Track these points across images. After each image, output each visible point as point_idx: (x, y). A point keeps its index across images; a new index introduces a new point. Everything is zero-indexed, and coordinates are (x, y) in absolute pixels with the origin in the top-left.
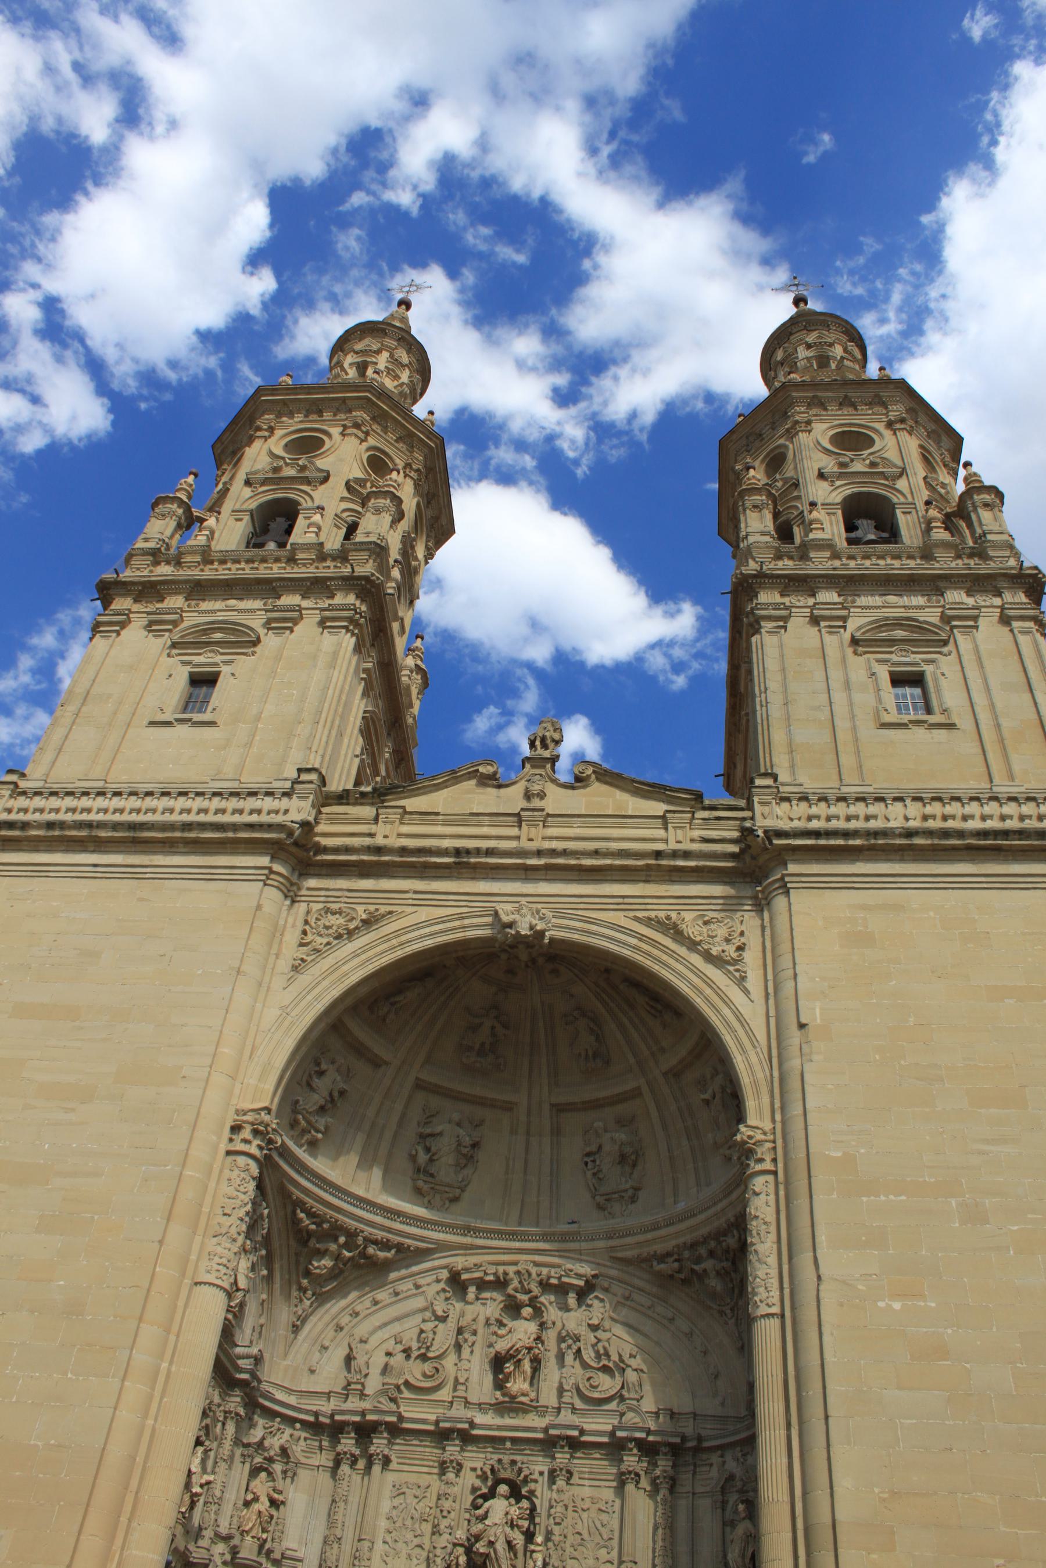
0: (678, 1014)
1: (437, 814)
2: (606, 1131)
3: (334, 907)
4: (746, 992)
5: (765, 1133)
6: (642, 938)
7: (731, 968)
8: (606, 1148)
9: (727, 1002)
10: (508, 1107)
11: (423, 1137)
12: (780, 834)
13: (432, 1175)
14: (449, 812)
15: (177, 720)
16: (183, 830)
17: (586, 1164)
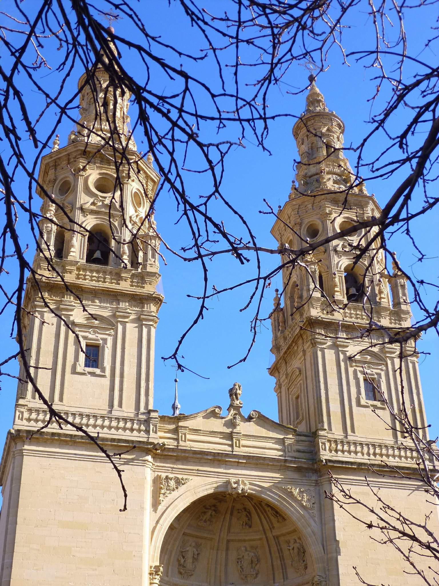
0: (284, 519)
1: (200, 430)
2: (246, 550)
3: (171, 476)
4: (315, 521)
5: (323, 578)
6: (280, 496)
7: (311, 512)
8: (246, 557)
9: (309, 526)
10: (211, 539)
11: (182, 552)
12: (330, 461)
13: (185, 567)
14: (205, 430)
15: (88, 372)
16: (111, 442)
17: (238, 562)
